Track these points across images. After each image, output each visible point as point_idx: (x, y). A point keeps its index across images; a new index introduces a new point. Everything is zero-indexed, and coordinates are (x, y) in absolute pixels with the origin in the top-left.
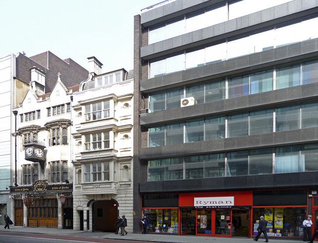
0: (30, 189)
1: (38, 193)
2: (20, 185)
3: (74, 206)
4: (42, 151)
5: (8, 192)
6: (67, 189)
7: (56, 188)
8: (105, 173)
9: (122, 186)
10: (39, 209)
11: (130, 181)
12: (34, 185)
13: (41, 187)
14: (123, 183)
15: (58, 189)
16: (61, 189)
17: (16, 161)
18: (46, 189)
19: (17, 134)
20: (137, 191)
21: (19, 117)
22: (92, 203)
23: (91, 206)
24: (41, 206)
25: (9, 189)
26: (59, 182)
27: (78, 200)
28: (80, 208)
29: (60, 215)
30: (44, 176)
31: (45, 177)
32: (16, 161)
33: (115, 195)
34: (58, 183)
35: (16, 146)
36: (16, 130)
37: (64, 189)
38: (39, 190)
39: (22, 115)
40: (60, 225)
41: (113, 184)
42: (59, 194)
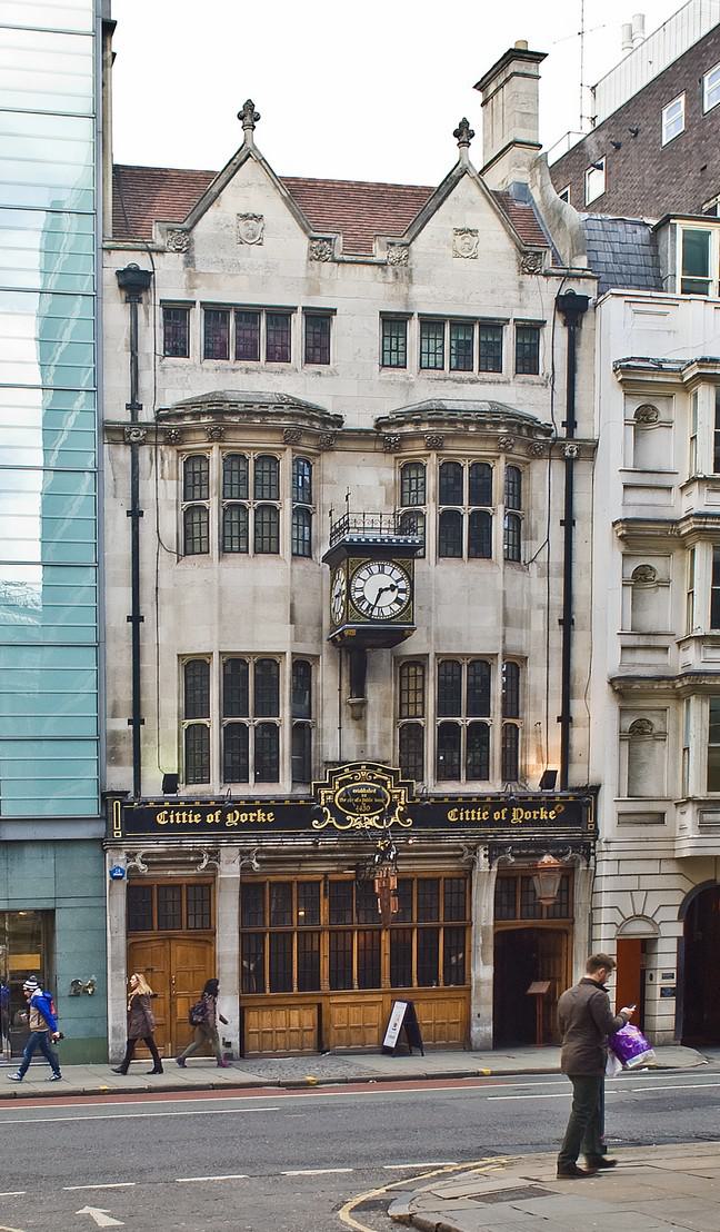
0: (291, 815)
2: (185, 791)
6: (550, 822)
15: (490, 822)
16: (500, 823)
18: (403, 816)
27: (632, 883)
31: (373, 739)
34: (477, 788)
36: (134, 407)
37: (525, 823)
38: (354, 822)
42: (495, 851)
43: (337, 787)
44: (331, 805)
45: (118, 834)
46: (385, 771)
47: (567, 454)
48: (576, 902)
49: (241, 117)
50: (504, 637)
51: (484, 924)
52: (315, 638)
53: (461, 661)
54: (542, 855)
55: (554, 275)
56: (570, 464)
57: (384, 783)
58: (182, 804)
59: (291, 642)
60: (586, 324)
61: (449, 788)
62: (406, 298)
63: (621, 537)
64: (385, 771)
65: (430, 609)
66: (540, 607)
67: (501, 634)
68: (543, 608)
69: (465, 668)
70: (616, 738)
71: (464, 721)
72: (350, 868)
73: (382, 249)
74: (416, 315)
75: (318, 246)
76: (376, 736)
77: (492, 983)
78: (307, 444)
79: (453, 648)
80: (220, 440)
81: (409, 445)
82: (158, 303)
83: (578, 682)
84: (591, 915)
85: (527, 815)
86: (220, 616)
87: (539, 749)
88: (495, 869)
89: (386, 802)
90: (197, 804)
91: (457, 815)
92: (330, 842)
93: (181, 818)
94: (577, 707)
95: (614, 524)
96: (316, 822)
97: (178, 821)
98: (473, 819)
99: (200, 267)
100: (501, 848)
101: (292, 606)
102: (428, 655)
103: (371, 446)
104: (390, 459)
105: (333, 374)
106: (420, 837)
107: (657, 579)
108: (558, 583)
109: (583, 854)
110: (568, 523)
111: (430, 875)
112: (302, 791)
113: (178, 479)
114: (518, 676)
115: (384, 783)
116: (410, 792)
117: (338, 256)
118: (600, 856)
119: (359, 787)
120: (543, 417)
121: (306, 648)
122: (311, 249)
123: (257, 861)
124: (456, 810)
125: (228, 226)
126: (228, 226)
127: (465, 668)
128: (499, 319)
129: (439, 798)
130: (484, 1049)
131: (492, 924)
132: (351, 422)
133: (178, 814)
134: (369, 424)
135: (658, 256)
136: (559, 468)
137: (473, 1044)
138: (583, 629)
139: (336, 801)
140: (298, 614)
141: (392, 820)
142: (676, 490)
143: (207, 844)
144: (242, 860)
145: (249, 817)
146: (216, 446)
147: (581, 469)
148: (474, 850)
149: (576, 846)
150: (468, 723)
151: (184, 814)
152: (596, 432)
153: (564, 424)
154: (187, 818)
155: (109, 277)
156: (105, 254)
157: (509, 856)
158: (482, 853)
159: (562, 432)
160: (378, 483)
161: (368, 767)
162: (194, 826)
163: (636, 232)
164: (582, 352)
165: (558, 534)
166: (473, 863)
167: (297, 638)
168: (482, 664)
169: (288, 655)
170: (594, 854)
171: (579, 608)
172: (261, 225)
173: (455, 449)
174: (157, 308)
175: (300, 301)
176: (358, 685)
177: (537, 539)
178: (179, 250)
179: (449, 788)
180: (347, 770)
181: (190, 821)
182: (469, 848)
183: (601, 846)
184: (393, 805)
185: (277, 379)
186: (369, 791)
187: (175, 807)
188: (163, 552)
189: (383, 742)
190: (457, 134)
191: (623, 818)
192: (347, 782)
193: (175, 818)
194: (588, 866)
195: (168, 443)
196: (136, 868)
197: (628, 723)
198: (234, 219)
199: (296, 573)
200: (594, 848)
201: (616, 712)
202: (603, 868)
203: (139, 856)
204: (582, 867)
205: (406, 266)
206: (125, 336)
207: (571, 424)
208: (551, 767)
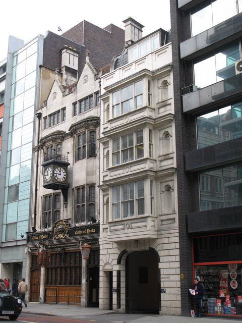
1: (58, 243)
3: (101, 263)
4: (64, 171)
5: (24, 243)
6: (93, 233)
8: (138, 200)
9: (164, 223)
10: (59, 270)
11: (174, 211)
12: (53, 227)
13: (62, 232)
14: (164, 218)
17: (36, 190)
19: (39, 148)
20: (185, 231)
21: (42, 121)
22: (124, 258)
23: (123, 262)
24: (62, 265)
25: (25, 237)
26: (82, 221)
28: (108, 267)
29: (84, 281)
30: (67, 212)
32: (36, 190)
33: (154, 240)
34: (83, 224)
37: (90, 233)
39: (45, 118)
40: (84, 300)
41: (149, 220)
67: (86, 178)
78: (58, 141)
130: (83, 307)
168: (83, 187)
176: (66, 199)
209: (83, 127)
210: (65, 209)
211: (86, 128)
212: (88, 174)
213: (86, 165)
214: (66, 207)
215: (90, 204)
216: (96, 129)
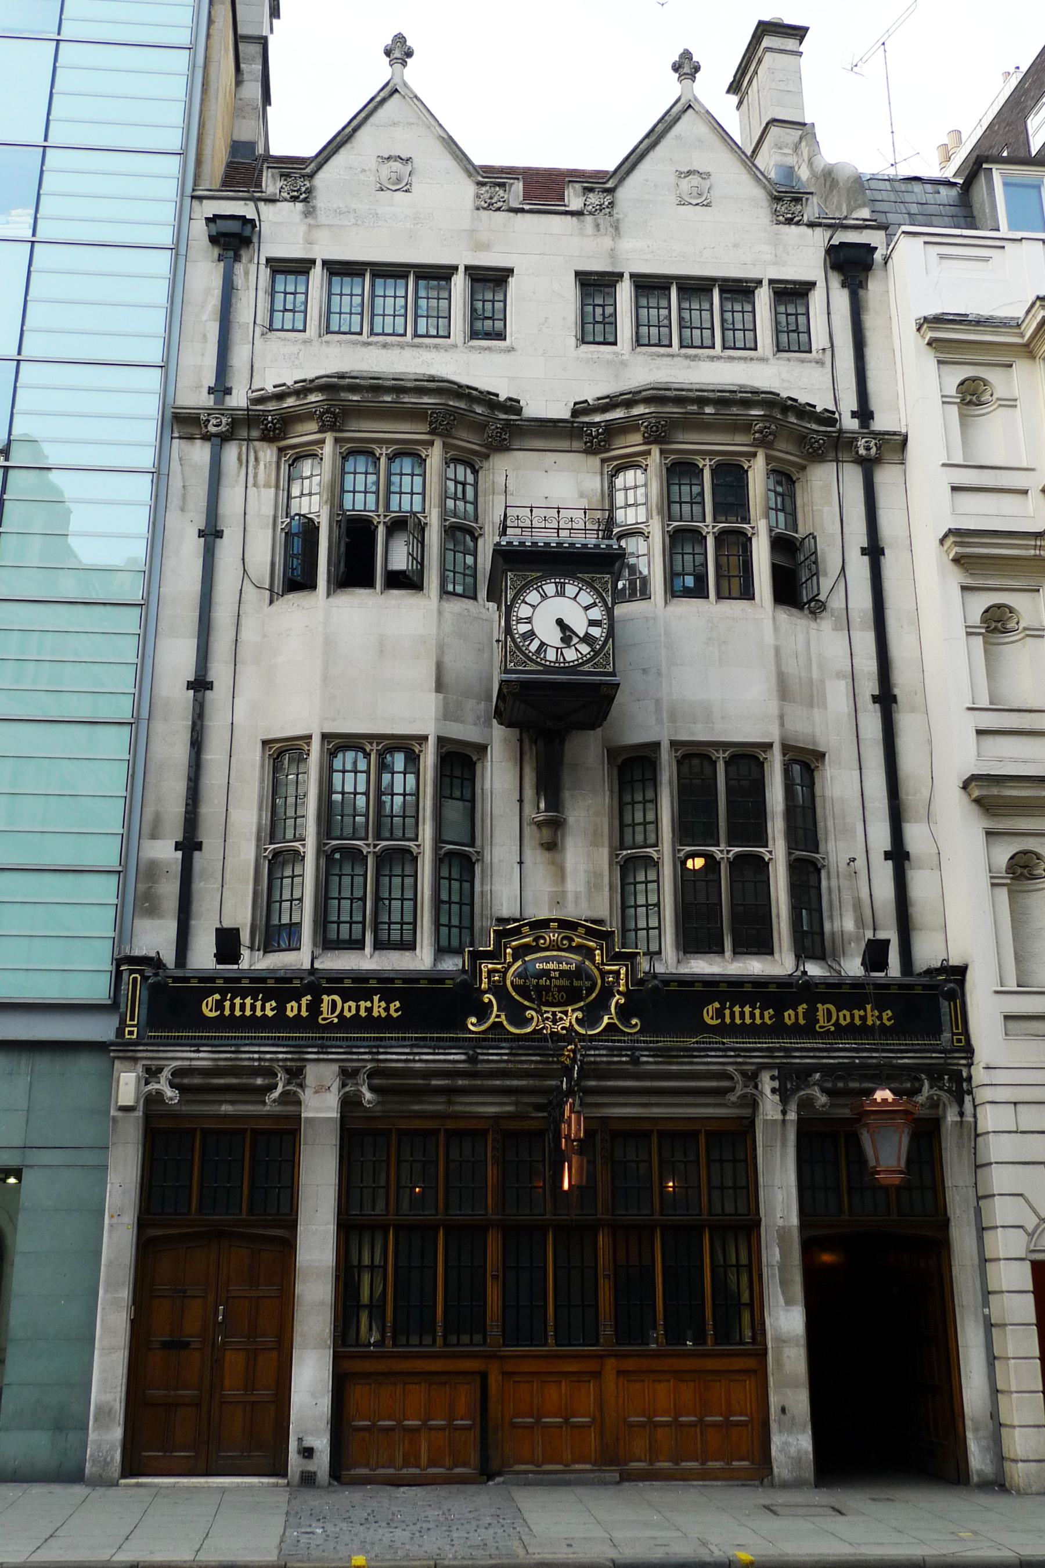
2: (252, 961)
7: (746, 1014)
13: (571, 996)
15: (778, 1029)
16: (795, 1030)
17: (200, 685)
30: (560, 873)
31: (576, 882)
32: (200, 685)
34: (755, 966)
35: (211, 534)
36: (221, 389)
37: (841, 1031)
38: (537, 1020)
43: (509, 959)
44: (498, 990)
45: (132, 1032)
46: (591, 933)
47: (862, 452)
48: (949, 1183)
49: (388, 53)
50: (781, 717)
51: (780, 1223)
52: (478, 718)
53: (715, 755)
54: (872, 1091)
55: (820, 225)
56: (868, 466)
57: (589, 953)
58: (245, 983)
59: (437, 719)
60: (874, 286)
61: (702, 966)
62: (613, 254)
63: (957, 560)
64: (591, 933)
65: (659, 673)
66: (839, 675)
68: (844, 677)
69: (721, 767)
70: (985, 882)
71: (723, 852)
72: (538, 1107)
73: (576, 195)
74: (627, 276)
75: (487, 192)
76: (582, 878)
77: (803, 1341)
79: (701, 734)
80: (333, 428)
81: (620, 441)
82: (263, 261)
83: (913, 794)
84: (978, 1211)
85: (844, 1017)
86: (326, 679)
87: (858, 906)
88: (792, 1116)
89: (590, 991)
90: (271, 984)
91: (719, 1013)
92: (495, 1056)
93: (243, 1007)
94: (915, 835)
95: (942, 541)
96: (474, 1020)
97: (238, 1013)
98: (748, 1021)
99: (322, 218)
100: (803, 1074)
101: (439, 667)
102: (657, 745)
103: (565, 444)
104: (595, 462)
105: (511, 349)
106: (657, 1052)
107: (1022, 625)
108: (865, 640)
109: (949, 1091)
110: (874, 551)
111: (681, 1127)
112: (451, 964)
113: (277, 487)
114: (814, 784)
115: (589, 953)
116: (633, 970)
117: (515, 205)
118: (983, 1095)
119: (547, 960)
120: (822, 402)
121: (466, 732)
122: (478, 196)
123: (371, 1089)
124: (717, 1005)
125: (364, 171)
126: (364, 171)
127: (721, 767)
128: (747, 281)
129: (688, 982)
130: (794, 1485)
131: (794, 1221)
132: (534, 408)
133: (238, 1001)
134: (562, 411)
135: (973, 217)
136: (853, 477)
137: (776, 1470)
138: (913, 710)
139: (508, 983)
140: (449, 677)
141: (606, 1020)
142: (1034, 494)
143: (281, 1053)
144: (344, 1085)
145: (358, 1008)
146: (329, 437)
147: (886, 477)
148: (752, 1078)
149: (935, 1074)
150: (731, 855)
151: (248, 1001)
152: (903, 423)
153: (854, 414)
154: (253, 1008)
155: (199, 230)
156: (196, 203)
157: (816, 1091)
158: (767, 1083)
159: (851, 424)
160: (576, 495)
161: (565, 925)
162: (262, 1023)
163: (939, 193)
164: (871, 321)
165: (859, 568)
166: (753, 1103)
167: (447, 714)
169: (432, 742)
170: (970, 1092)
171: (903, 680)
172: (409, 168)
173: (688, 442)
174: (262, 267)
175: (463, 257)
177: (826, 575)
178: (294, 199)
179: (702, 966)
180: (526, 929)
181: (259, 1013)
182: (744, 1074)
183: (979, 1075)
184: (607, 992)
185: (427, 356)
186: (564, 966)
187: (234, 987)
188: (248, 588)
189: (593, 887)
190: (676, 68)
191: (1012, 1025)
192: (526, 949)
193: (232, 1007)
194: (961, 1114)
195: (265, 438)
196: (159, 1093)
197: (1003, 854)
198: (373, 163)
199: (447, 616)
200: (970, 1078)
201: (981, 837)
202: (990, 1119)
203: (166, 1074)
204: (951, 1117)
205: (610, 215)
206: (214, 301)
207: (864, 414)
208: (882, 935)
209: (746, 427)
210: (535, 858)
211: (764, 442)
212: (784, 691)
213: (769, 638)
214: (552, 846)
215: (629, 859)
216: (803, 468)
